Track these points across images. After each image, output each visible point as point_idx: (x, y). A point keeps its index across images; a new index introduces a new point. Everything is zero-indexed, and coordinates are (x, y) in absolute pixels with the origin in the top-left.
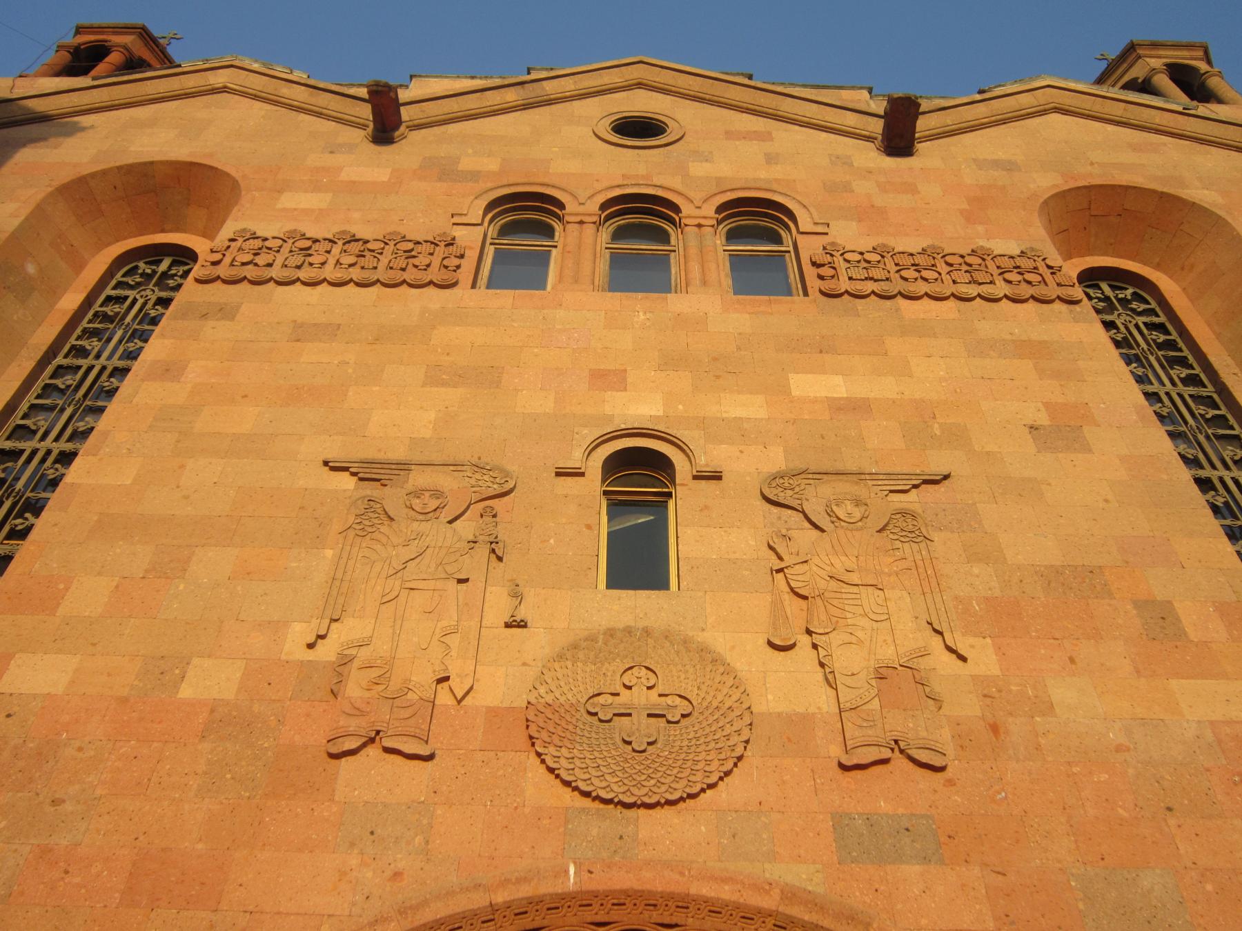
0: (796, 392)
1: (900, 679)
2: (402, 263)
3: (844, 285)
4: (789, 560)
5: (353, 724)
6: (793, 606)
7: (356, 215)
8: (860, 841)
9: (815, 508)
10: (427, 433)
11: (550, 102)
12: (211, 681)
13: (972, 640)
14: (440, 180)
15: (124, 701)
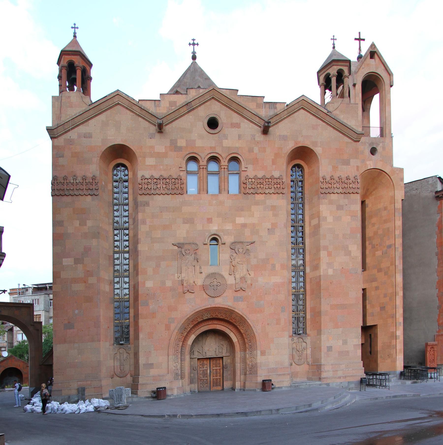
0: (237, 222)
1: (243, 279)
2: (173, 187)
3: (248, 191)
4: (233, 260)
5: (186, 289)
6: (232, 267)
7: (161, 167)
8: (236, 299)
9: (236, 250)
10: (185, 236)
11: (193, 109)
12: (169, 284)
13: (252, 272)
14: (175, 151)
15: (160, 287)
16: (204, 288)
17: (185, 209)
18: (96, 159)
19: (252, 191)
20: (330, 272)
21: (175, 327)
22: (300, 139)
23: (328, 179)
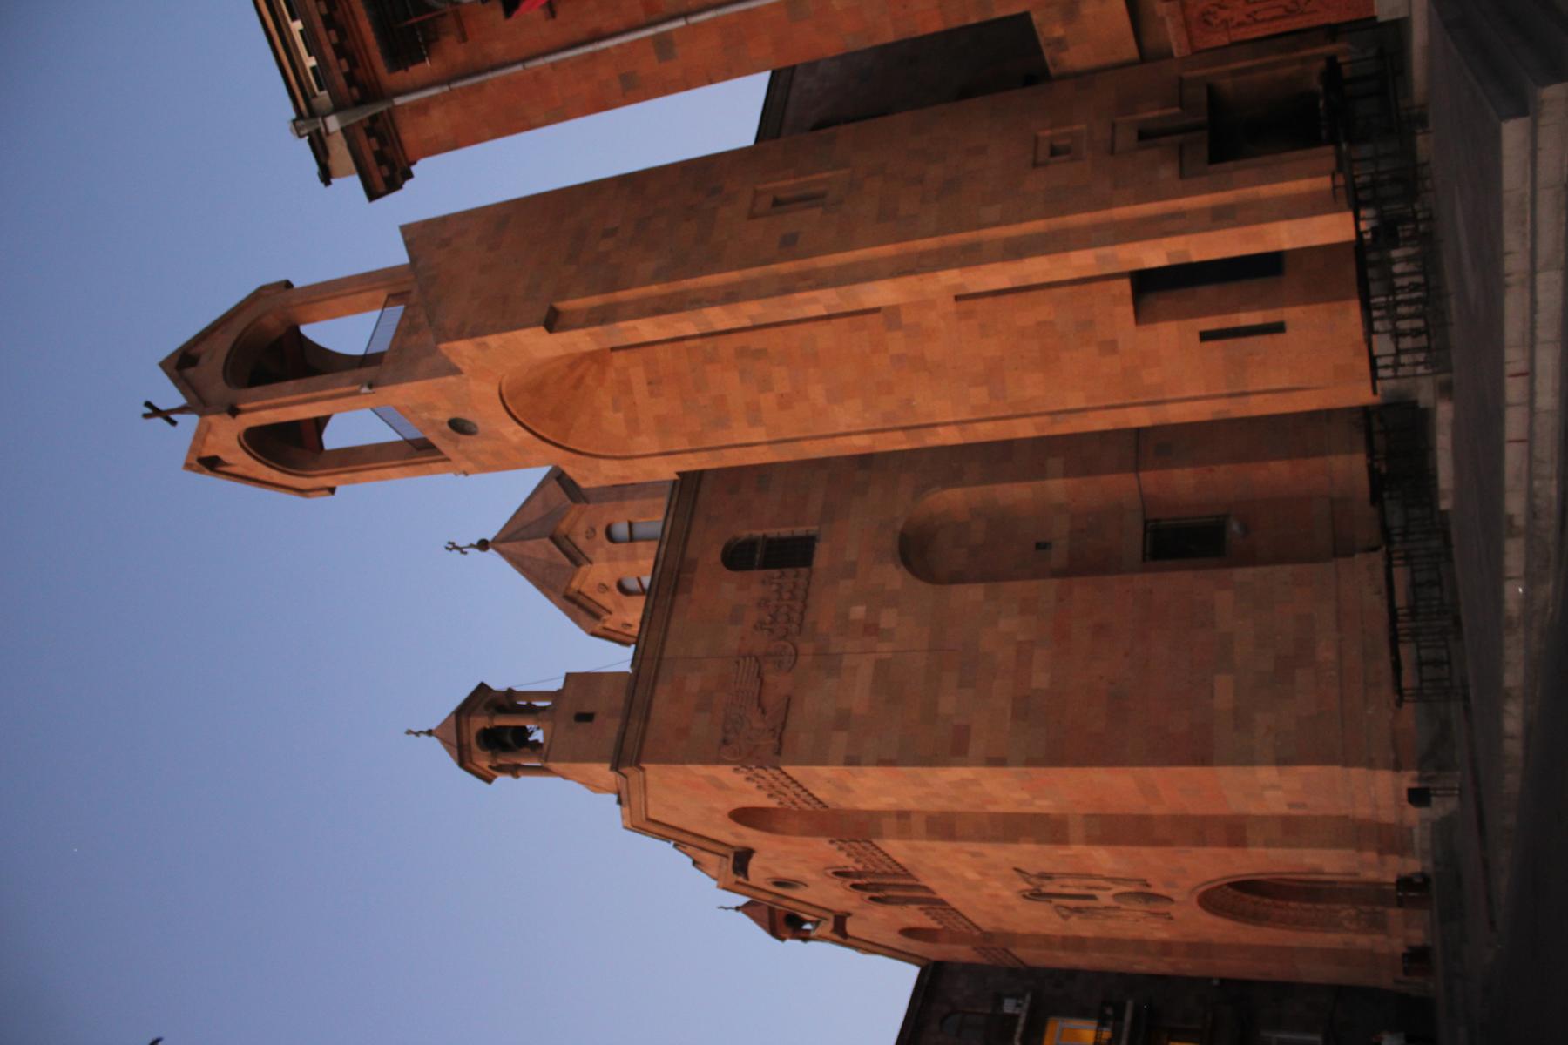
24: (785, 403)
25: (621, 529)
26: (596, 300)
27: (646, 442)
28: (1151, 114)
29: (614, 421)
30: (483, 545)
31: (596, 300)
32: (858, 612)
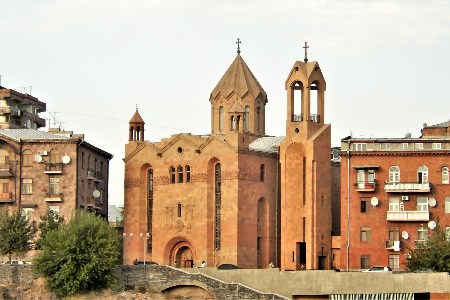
12: (163, 226)
16: (175, 227)
17: (170, 191)
18: (139, 171)
19: (194, 181)
20: (225, 219)
21: (165, 245)
22: (213, 154)
23: (224, 172)
24: (291, 187)
25: (248, 110)
26: (315, 168)
27: (288, 160)
28: (325, 249)
29: (292, 155)
30: (239, 52)
31: (315, 168)
32: (255, 191)
